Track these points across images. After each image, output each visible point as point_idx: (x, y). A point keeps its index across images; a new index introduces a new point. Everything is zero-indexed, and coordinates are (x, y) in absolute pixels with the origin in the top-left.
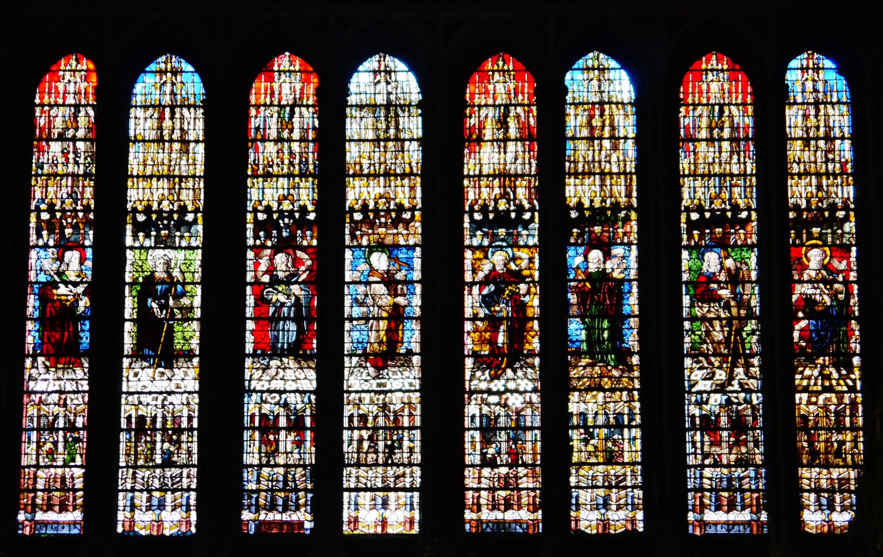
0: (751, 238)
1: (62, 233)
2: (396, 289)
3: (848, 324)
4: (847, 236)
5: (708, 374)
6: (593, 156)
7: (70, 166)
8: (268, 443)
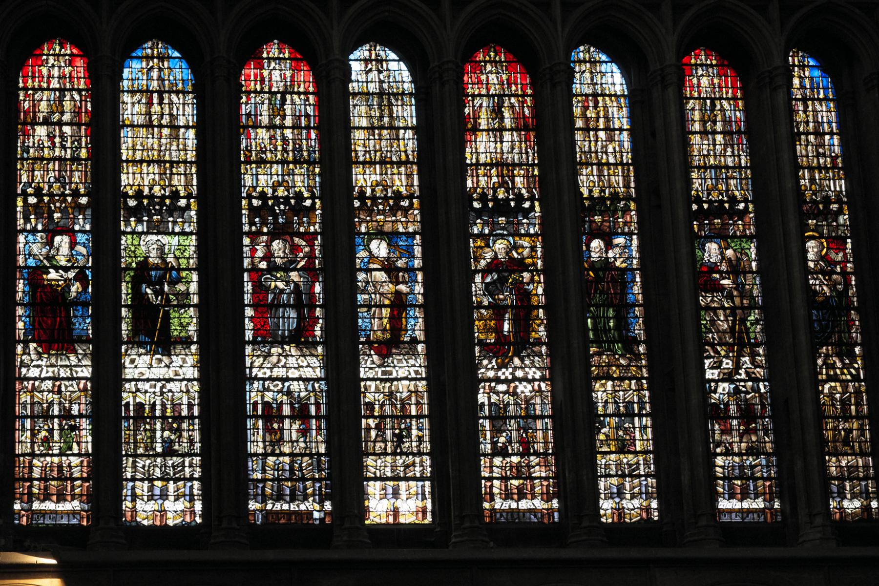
0: (750, 229)
1: (51, 217)
2: (397, 277)
3: (849, 314)
4: (842, 228)
5: (715, 363)
6: (590, 147)
7: (57, 150)
8: (271, 431)
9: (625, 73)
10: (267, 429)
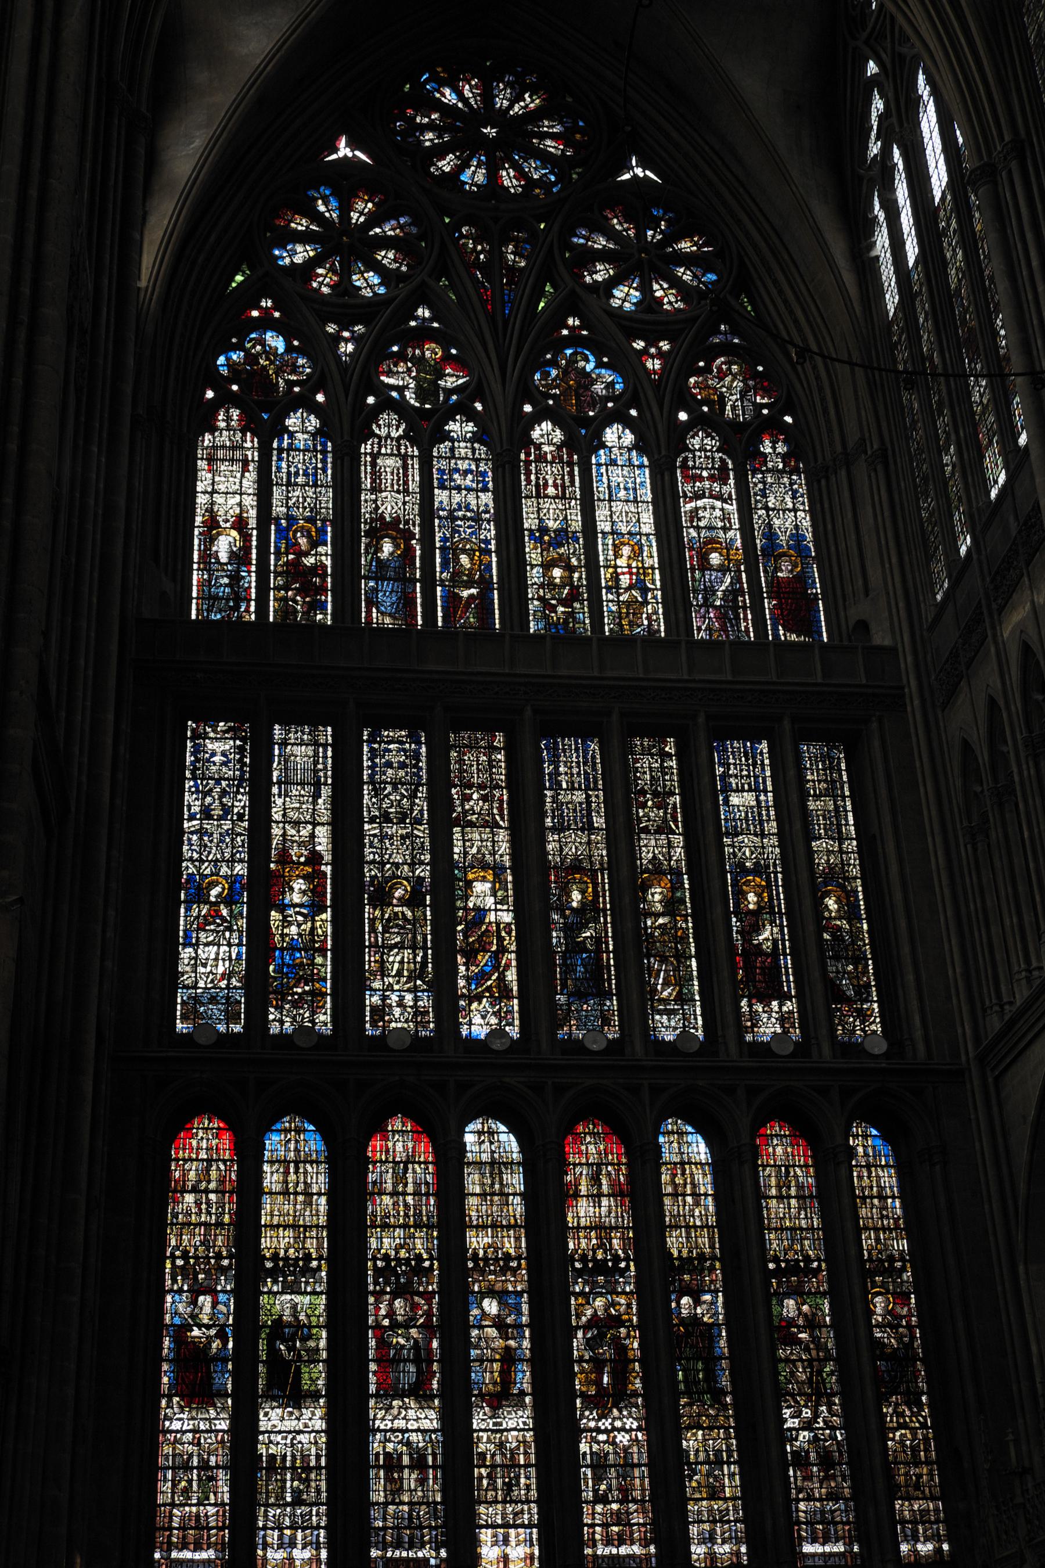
1: (196, 1278)
2: (507, 1332)
3: (914, 1366)
7: (203, 1216)
9: (708, 1144)
10: (388, 1479)
